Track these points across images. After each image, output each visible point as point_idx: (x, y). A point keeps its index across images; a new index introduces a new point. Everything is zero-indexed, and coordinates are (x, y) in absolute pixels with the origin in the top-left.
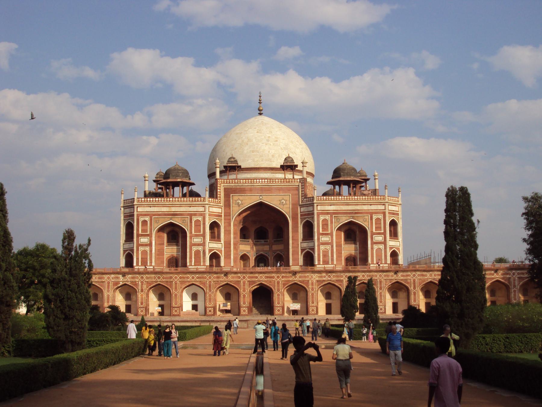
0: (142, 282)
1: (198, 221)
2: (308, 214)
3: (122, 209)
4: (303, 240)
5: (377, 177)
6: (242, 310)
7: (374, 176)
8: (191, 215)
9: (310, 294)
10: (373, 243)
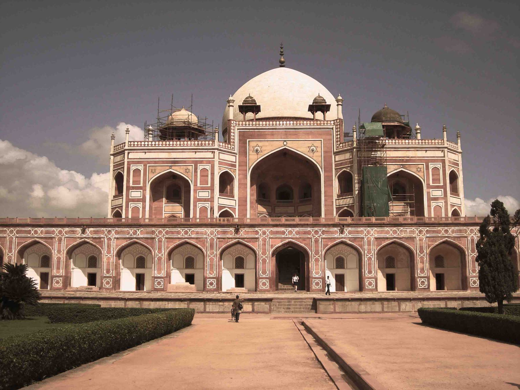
0: (109, 239)
1: (204, 170)
2: (346, 163)
3: (112, 157)
4: (338, 196)
5: (419, 131)
6: (261, 282)
7: (417, 130)
8: (196, 163)
9: (365, 259)
10: (430, 199)
